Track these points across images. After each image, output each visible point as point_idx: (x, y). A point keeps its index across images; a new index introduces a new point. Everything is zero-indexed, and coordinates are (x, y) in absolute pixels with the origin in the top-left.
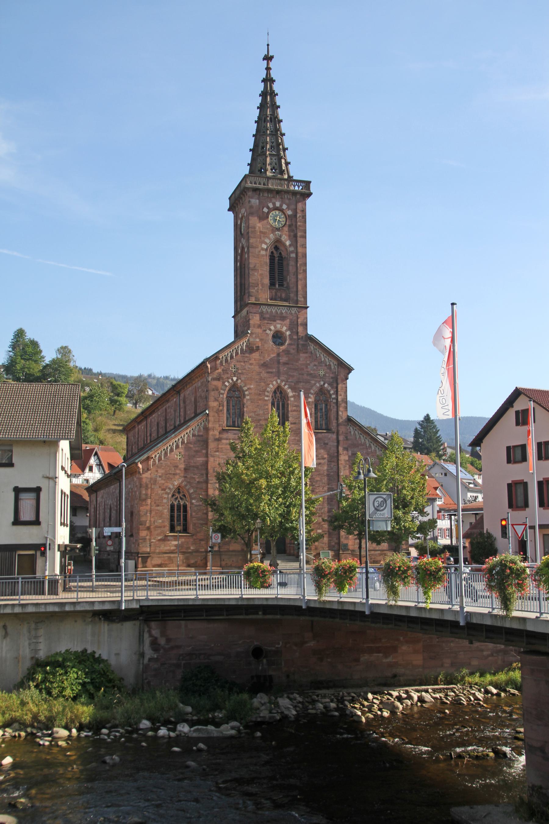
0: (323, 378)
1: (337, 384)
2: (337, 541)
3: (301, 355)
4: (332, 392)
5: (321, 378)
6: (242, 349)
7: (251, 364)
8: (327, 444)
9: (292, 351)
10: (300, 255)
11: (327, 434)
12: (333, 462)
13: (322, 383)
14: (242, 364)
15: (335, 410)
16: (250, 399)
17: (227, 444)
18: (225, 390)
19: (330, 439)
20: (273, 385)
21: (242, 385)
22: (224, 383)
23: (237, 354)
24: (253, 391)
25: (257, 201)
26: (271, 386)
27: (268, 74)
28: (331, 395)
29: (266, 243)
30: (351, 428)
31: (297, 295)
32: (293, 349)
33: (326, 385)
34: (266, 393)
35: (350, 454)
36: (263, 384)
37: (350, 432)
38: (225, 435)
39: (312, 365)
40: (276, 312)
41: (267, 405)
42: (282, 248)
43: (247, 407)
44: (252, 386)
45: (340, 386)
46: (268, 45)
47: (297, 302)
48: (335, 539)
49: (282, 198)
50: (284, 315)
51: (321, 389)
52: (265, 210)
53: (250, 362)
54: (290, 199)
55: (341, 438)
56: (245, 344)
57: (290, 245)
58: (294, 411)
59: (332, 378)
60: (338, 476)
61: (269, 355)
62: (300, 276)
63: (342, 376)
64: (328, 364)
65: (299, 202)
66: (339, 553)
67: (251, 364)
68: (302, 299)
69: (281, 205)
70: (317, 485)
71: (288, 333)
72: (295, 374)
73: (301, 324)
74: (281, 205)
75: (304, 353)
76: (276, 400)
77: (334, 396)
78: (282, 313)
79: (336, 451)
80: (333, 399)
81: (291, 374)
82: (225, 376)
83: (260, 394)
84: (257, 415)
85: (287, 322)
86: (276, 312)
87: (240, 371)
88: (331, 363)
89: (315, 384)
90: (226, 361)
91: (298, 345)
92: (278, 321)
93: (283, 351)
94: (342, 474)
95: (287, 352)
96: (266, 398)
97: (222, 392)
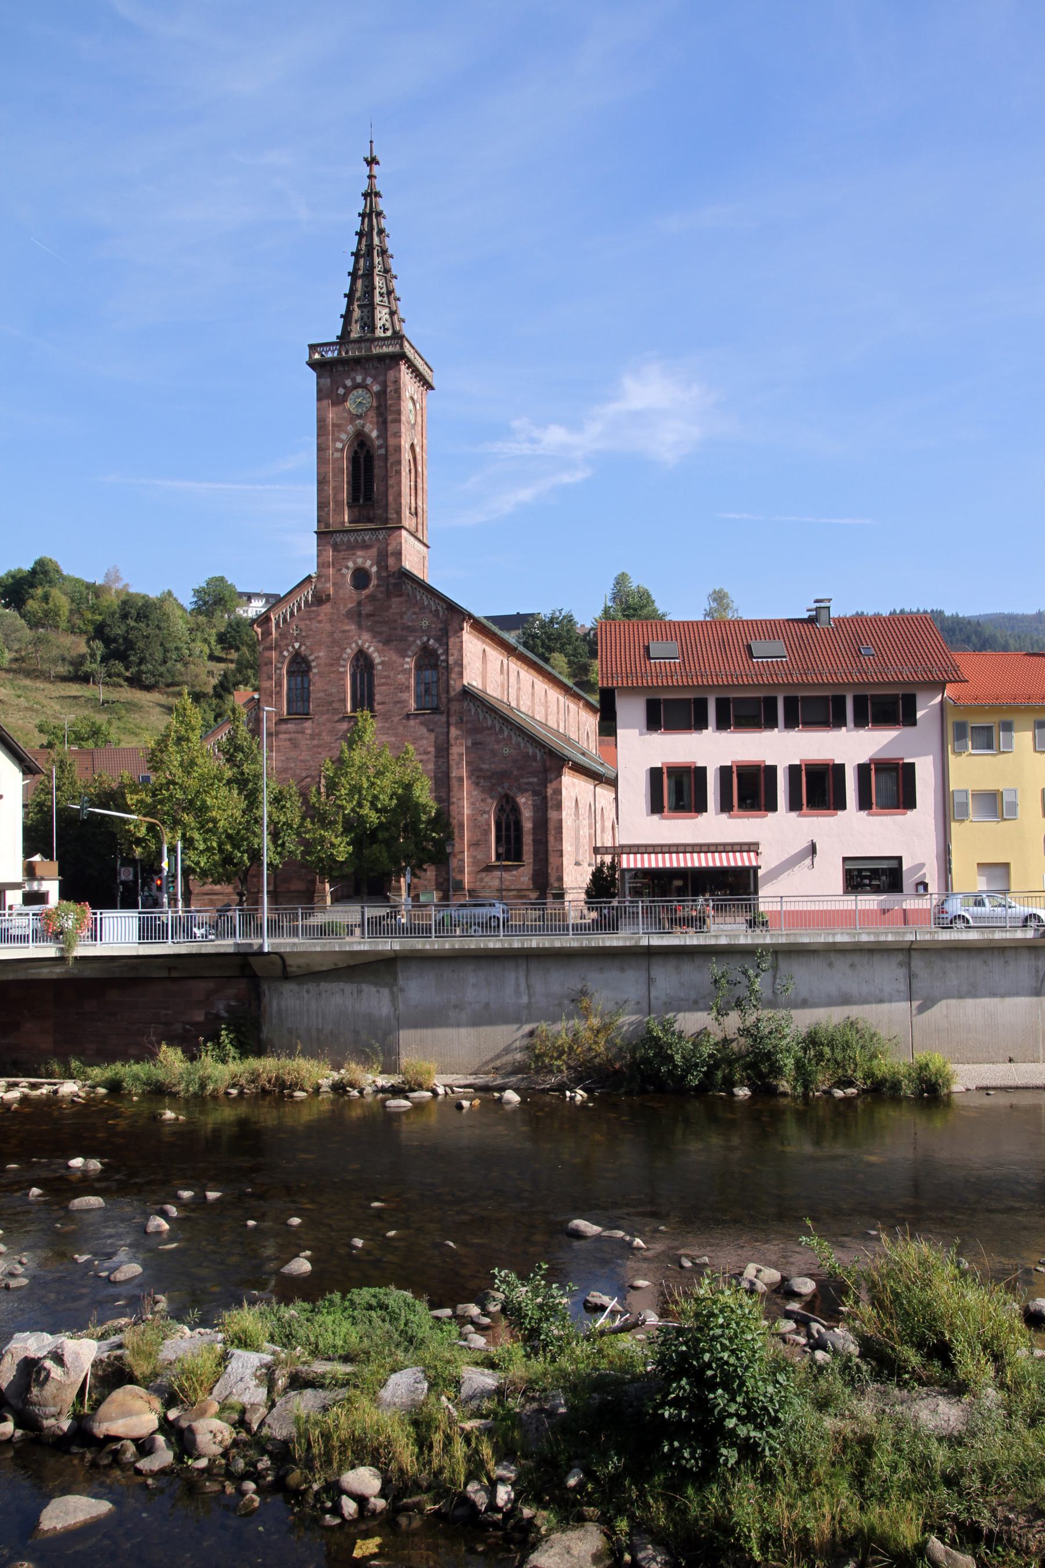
0: (427, 631)
1: (448, 638)
3: (393, 600)
4: (440, 651)
5: (423, 631)
6: (306, 601)
7: (320, 622)
9: (380, 596)
10: (391, 449)
11: (431, 716)
12: (442, 757)
13: (425, 639)
14: (308, 622)
15: (445, 678)
16: (319, 673)
17: (286, 740)
18: (283, 663)
19: (436, 723)
20: (351, 649)
21: (308, 653)
22: (281, 652)
23: (299, 608)
24: (322, 661)
25: (328, 380)
26: (349, 651)
27: (371, 185)
28: (438, 656)
29: (341, 441)
30: (471, 704)
31: (386, 511)
32: (382, 592)
33: (431, 642)
34: (342, 662)
35: (469, 744)
36: (336, 649)
37: (470, 710)
38: (284, 727)
39: (409, 613)
40: (356, 541)
41: (343, 679)
42: (368, 443)
43: (314, 684)
44: (321, 654)
45: (452, 641)
46: (371, 142)
47: (386, 521)
49: (365, 369)
50: (368, 542)
51: (425, 648)
52: (341, 391)
53: (319, 618)
54: (377, 368)
55: (453, 720)
56: (311, 592)
57: (378, 437)
58: (383, 684)
59: (440, 630)
60: (448, 777)
61: (345, 606)
62: (391, 482)
63: (455, 625)
64: (433, 609)
65: (390, 369)
67: (320, 622)
68: (395, 516)
69: (364, 380)
71: (374, 569)
72: (384, 629)
73: (393, 554)
74: (364, 380)
75: (397, 596)
76: (358, 671)
77: (443, 658)
78: (364, 541)
80: (443, 661)
81: (378, 630)
82: (283, 643)
83: (332, 665)
85: (374, 551)
86: (356, 541)
87: (304, 634)
88: (439, 608)
89: (414, 641)
90: (285, 619)
91: (388, 585)
92: (359, 553)
93: (367, 597)
94: (453, 775)
95: (372, 598)
96: (341, 669)
97: (279, 665)
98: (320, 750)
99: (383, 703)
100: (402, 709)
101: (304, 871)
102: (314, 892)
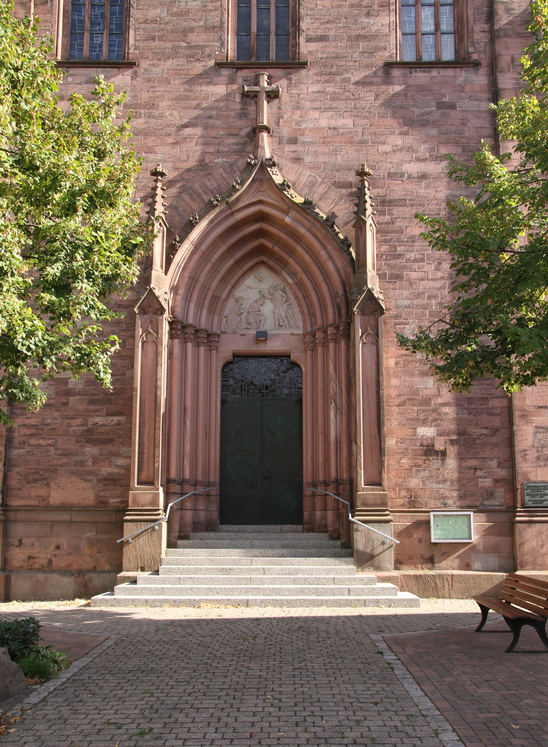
2: (502, 473)
8: (452, 106)
48: (494, 463)
66: (513, 523)
70: (412, 256)
79: (489, 131)
84: (181, 14)
98: (151, 141)
99: (323, 38)
100: (371, 53)
101: (90, 450)
102: (123, 510)
